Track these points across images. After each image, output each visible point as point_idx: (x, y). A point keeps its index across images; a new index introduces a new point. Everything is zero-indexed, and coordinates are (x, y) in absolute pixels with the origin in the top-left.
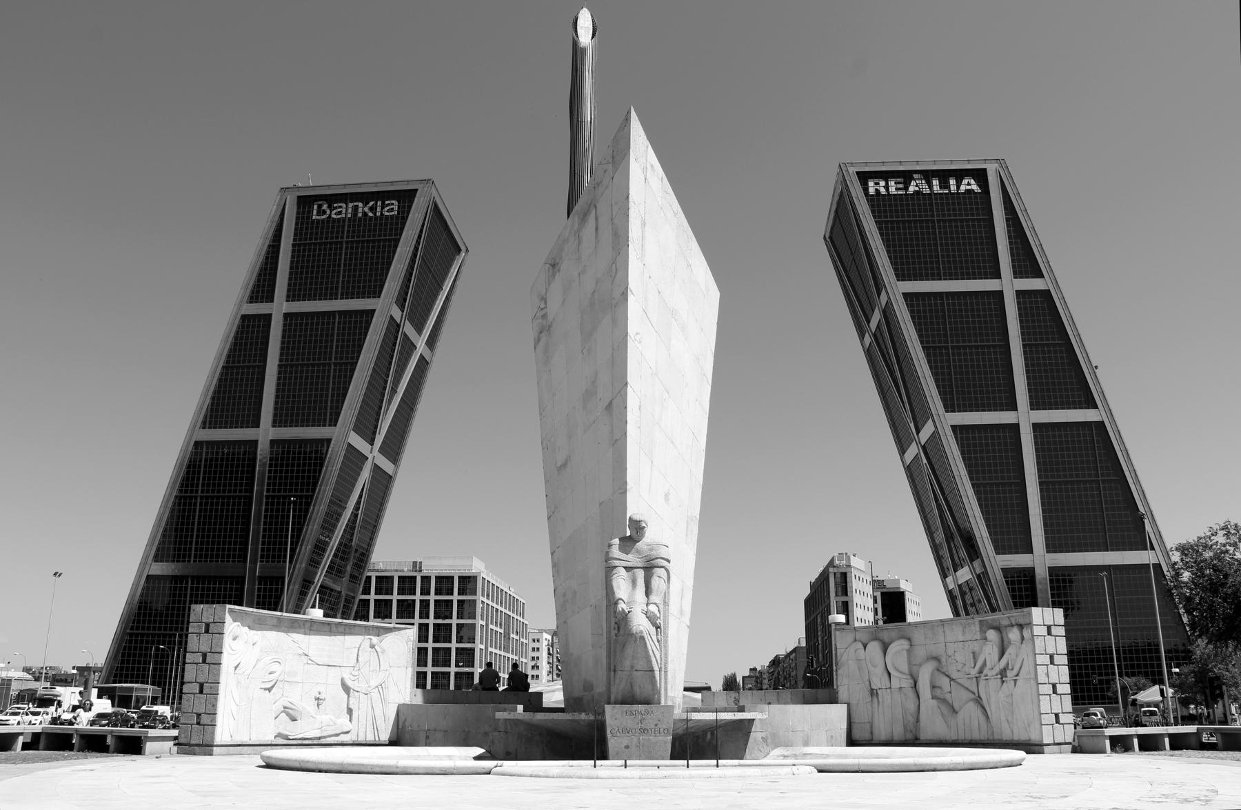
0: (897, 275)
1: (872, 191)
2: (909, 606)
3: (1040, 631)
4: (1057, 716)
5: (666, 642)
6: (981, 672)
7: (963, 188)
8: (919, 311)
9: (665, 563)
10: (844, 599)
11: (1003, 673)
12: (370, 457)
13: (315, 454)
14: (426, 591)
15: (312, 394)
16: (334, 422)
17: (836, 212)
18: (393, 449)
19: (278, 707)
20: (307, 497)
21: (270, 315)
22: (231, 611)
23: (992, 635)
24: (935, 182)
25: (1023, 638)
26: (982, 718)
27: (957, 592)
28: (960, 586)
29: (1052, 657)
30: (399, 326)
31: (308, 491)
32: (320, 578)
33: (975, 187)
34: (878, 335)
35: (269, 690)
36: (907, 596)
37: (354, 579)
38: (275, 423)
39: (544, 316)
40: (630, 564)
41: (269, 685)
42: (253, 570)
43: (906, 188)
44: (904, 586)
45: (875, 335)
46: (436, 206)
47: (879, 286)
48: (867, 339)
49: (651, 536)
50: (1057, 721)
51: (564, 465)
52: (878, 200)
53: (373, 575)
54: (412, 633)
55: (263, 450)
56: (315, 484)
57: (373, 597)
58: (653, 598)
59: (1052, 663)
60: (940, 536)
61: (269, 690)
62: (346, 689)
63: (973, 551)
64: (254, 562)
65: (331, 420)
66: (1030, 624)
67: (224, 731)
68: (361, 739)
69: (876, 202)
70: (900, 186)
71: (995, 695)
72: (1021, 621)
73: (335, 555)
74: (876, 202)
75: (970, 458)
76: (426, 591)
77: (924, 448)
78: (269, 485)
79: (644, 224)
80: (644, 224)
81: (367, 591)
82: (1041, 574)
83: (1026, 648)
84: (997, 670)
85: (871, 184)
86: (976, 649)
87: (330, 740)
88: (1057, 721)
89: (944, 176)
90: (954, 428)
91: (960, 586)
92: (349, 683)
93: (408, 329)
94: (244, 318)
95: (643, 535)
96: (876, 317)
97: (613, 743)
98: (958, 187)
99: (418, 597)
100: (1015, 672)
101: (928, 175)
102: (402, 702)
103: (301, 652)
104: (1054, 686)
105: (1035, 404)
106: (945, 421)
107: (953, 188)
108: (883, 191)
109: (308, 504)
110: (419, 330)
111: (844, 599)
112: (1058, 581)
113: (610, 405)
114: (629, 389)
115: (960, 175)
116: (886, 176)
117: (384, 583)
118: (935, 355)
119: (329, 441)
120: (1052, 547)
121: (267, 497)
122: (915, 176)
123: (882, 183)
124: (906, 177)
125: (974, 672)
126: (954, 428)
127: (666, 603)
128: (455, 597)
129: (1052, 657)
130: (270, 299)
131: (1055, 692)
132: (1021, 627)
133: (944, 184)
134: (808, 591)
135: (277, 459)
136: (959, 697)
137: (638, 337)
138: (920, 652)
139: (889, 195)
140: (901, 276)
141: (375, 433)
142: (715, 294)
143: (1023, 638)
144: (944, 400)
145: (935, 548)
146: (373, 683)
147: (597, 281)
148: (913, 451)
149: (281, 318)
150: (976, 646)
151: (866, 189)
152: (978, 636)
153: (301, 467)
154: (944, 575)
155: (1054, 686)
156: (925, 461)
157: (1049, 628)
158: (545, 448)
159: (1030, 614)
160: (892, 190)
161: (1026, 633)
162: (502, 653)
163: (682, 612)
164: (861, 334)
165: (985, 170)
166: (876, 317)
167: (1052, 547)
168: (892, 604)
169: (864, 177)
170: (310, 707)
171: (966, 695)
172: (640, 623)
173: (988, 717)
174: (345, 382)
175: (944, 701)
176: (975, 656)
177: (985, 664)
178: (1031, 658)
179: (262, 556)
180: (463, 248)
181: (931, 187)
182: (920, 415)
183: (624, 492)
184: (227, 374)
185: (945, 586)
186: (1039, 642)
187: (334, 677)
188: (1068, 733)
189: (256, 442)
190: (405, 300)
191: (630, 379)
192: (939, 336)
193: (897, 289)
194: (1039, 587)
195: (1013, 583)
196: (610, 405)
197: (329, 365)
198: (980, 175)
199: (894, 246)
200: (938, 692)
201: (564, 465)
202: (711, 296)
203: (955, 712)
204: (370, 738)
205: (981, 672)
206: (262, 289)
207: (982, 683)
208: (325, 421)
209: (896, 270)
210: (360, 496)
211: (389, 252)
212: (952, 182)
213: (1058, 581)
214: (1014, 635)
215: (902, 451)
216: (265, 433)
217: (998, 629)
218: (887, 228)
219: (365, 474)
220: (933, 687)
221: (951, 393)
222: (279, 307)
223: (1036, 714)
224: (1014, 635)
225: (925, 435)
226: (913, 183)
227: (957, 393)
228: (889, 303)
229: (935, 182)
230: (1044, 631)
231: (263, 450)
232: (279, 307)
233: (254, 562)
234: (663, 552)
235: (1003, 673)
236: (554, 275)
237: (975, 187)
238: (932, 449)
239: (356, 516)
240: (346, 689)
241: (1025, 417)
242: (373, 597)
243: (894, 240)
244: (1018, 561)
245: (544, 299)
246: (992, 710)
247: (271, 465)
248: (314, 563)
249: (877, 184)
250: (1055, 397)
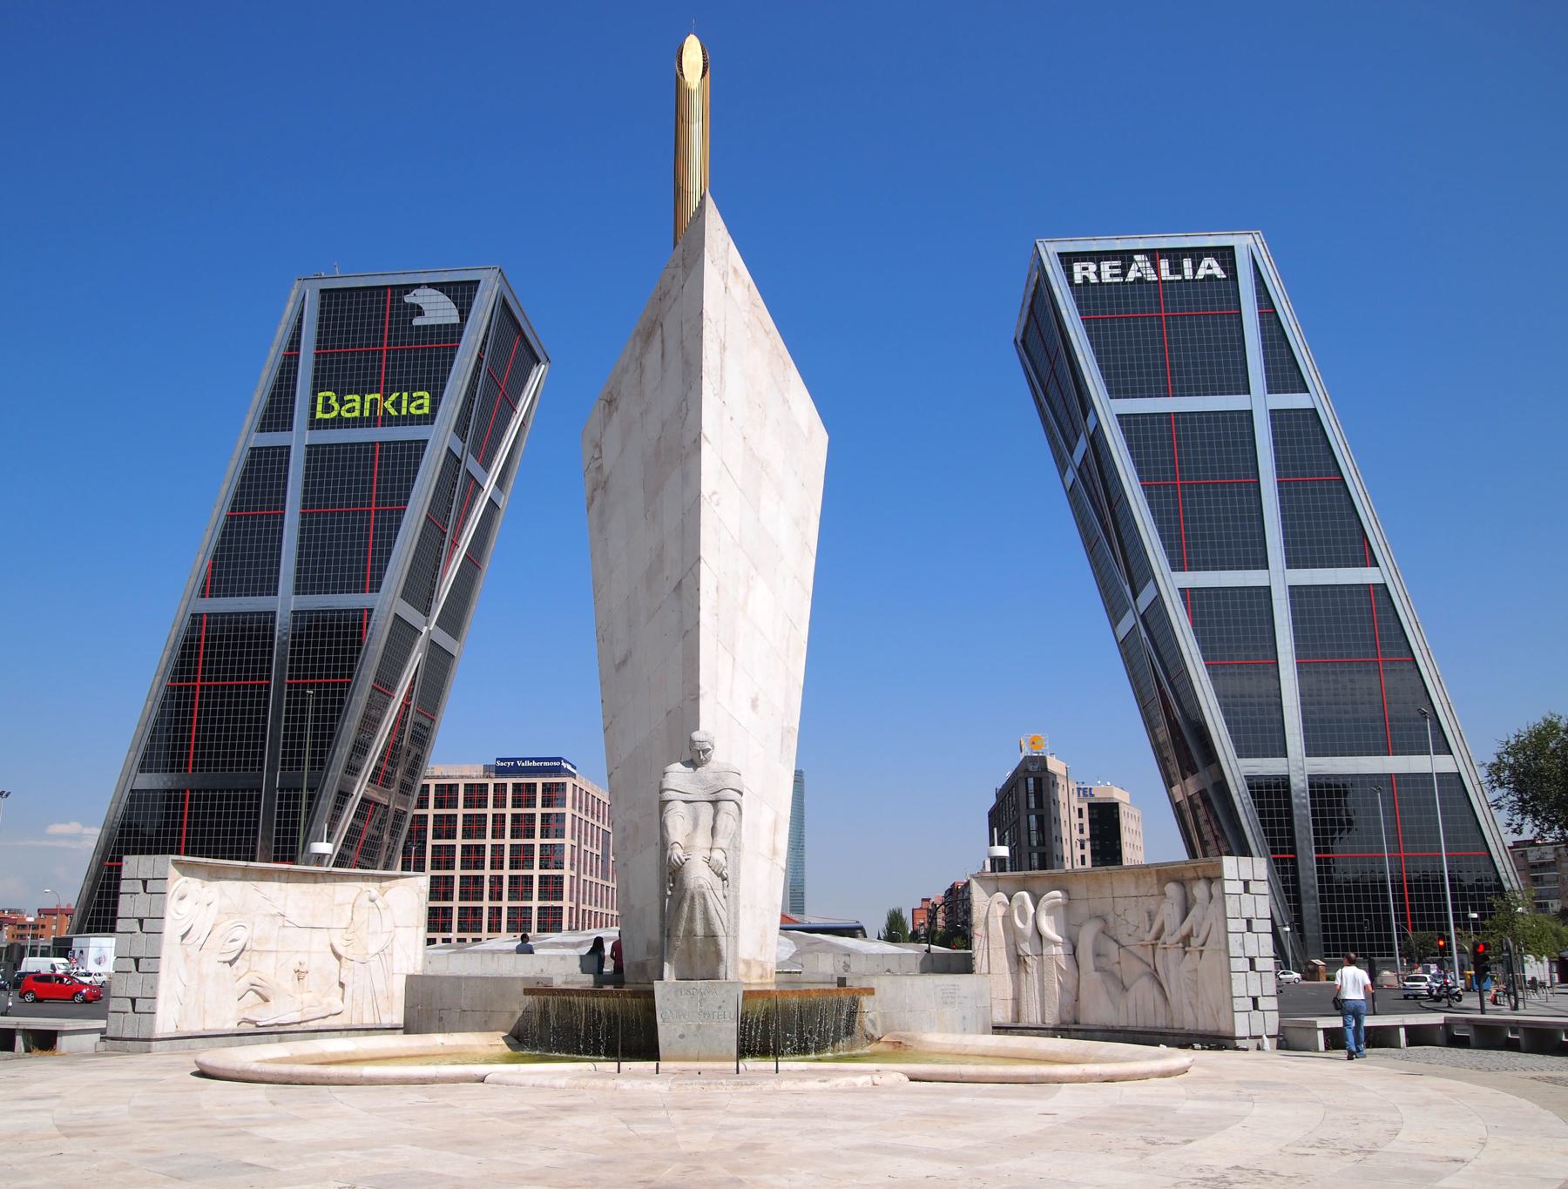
0: (1109, 391)
1: (1078, 279)
2: (1124, 822)
3: (1234, 887)
4: (1255, 1000)
5: (736, 897)
6: (1158, 938)
8: (1138, 439)
9: (736, 796)
10: (1040, 812)
11: (1186, 940)
12: (425, 630)
13: (352, 628)
14: (500, 802)
15: (348, 552)
16: (376, 587)
17: (1031, 306)
18: (453, 621)
19: (244, 983)
20: (342, 685)
21: (289, 447)
22: (176, 863)
23: (1172, 889)
25: (1211, 897)
26: (1159, 999)
27: (1186, 805)
28: (1190, 798)
29: (1249, 922)
30: (459, 461)
31: (342, 676)
32: (361, 788)
34: (1085, 470)
35: (231, 963)
36: (1123, 809)
37: (406, 789)
38: (300, 589)
39: (600, 468)
40: (690, 798)
41: (230, 957)
42: (271, 780)
43: (1124, 275)
44: (1119, 795)
45: (1079, 470)
46: (505, 303)
47: (1086, 404)
48: (1070, 476)
49: (718, 758)
50: (1255, 1007)
51: (624, 662)
52: (1087, 291)
53: (432, 783)
54: (421, 883)
55: (283, 626)
56: (351, 668)
57: (431, 811)
58: (722, 841)
59: (1249, 929)
60: (1163, 734)
61: (231, 963)
62: (338, 957)
63: (1210, 756)
64: (272, 770)
65: (372, 584)
66: (1220, 878)
67: (165, 1023)
68: (355, 1023)
69: (1084, 293)
71: (1175, 969)
72: (1211, 874)
73: (381, 759)
74: (1084, 293)
75: (1203, 632)
76: (500, 802)
77: (1143, 617)
78: (291, 669)
79: (723, 348)
80: (723, 348)
81: (423, 803)
82: (1299, 784)
83: (1214, 908)
84: (1178, 936)
85: (1077, 267)
86: (1153, 907)
87: (313, 1025)
88: (1255, 1007)
90: (1183, 591)
91: (1190, 798)
92: (340, 950)
93: (472, 464)
94: (255, 452)
95: (707, 761)
96: (1082, 445)
97: (666, 1033)
99: (490, 811)
100: (1201, 940)
102: (411, 972)
103: (275, 911)
104: (1252, 960)
105: (1293, 562)
106: (1171, 583)
108: (1093, 279)
109: (342, 694)
110: (487, 466)
111: (1040, 812)
112: (1321, 794)
113: (678, 587)
114: (703, 565)
116: (1097, 257)
117: (446, 794)
118: (1159, 496)
119: (371, 610)
120: (1312, 749)
121: (290, 686)
123: (1092, 267)
125: (1149, 937)
126: (1183, 591)
127: (737, 848)
128: (539, 810)
129: (1249, 922)
130: (287, 425)
131: (1252, 968)
132: (1210, 880)
134: (992, 801)
135: (301, 636)
136: (1132, 969)
137: (715, 498)
138: (1082, 909)
139: (1101, 283)
140: (1115, 392)
141: (430, 600)
142: (821, 439)
143: (1211, 897)
144: (1170, 556)
145: (1158, 748)
146: (373, 949)
147: (664, 425)
148: (1128, 621)
149: (303, 450)
150: (1152, 904)
151: (1070, 276)
152: (1155, 891)
153: (332, 646)
154: (1169, 784)
155: (1252, 960)
156: (1144, 634)
157: (1246, 883)
158: (601, 639)
159: (1220, 866)
160: (1106, 277)
161: (1215, 889)
162: (600, 881)
163: (775, 852)
164: (1062, 471)
165: (1230, 250)
166: (1082, 445)
167: (1312, 749)
168: (1105, 820)
170: (287, 982)
171: (1138, 967)
172: (699, 875)
173: (1166, 998)
174: (389, 536)
175: (1112, 974)
176: (1151, 916)
177: (1162, 929)
178: (1221, 924)
179: (283, 763)
180: (542, 357)
182: (1139, 574)
183: (696, 699)
184: (232, 526)
185: (1171, 797)
186: (1231, 903)
187: (319, 942)
188: (1272, 1023)
189: (274, 613)
190: (467, 427)
191: (704, 553)
192: (1164, 471)
193: (1108, 409)
194: (1295, 801)
195: (1260, 795)
196: (678, 587)
197: (369, 512)
199: (1107, 352)
200: (1104, 960)
201: (624, 662)
202: (815, 441)
203: (1125, 989)
204: (368, 1021)
205: (1158, 938)
206: (277, 414)
207: (1159, 952)
208: (364, 585)
209: (1108, 384)
210: (413, 682)
211: (444, 364)
213: (1321, 794)
214: (1200, 890)
215: (1115, 620)
216: (285, 603)
217: (1181, 882)
218: (1097, 329)
219: (417, 657)
220: (1097, 955)
221: (1180, 546)
222: (299, 439)
223: (1227, 994)
224: (1200, 890)
225: (1144, 600)
227: (1188, 546)
228: (1098, 426)
230: (1239, 887)
231: (283, 626)
232: (299, 439)
233: (272, 770)
234: (732, 782)
235: (1186, 940)
236: (610, 415)
238: (1155, 616)
239: (408, 707)
240: (338, 957)
241: (1279, 577)
242: (431, 811)
243: (1106, 344)
244: (1268, 766)
245: (598, 446)
246: (1172, 988)
247: (293, 644)
248: (353, 770)
249: (1085, 269)
250: (1321, 551)
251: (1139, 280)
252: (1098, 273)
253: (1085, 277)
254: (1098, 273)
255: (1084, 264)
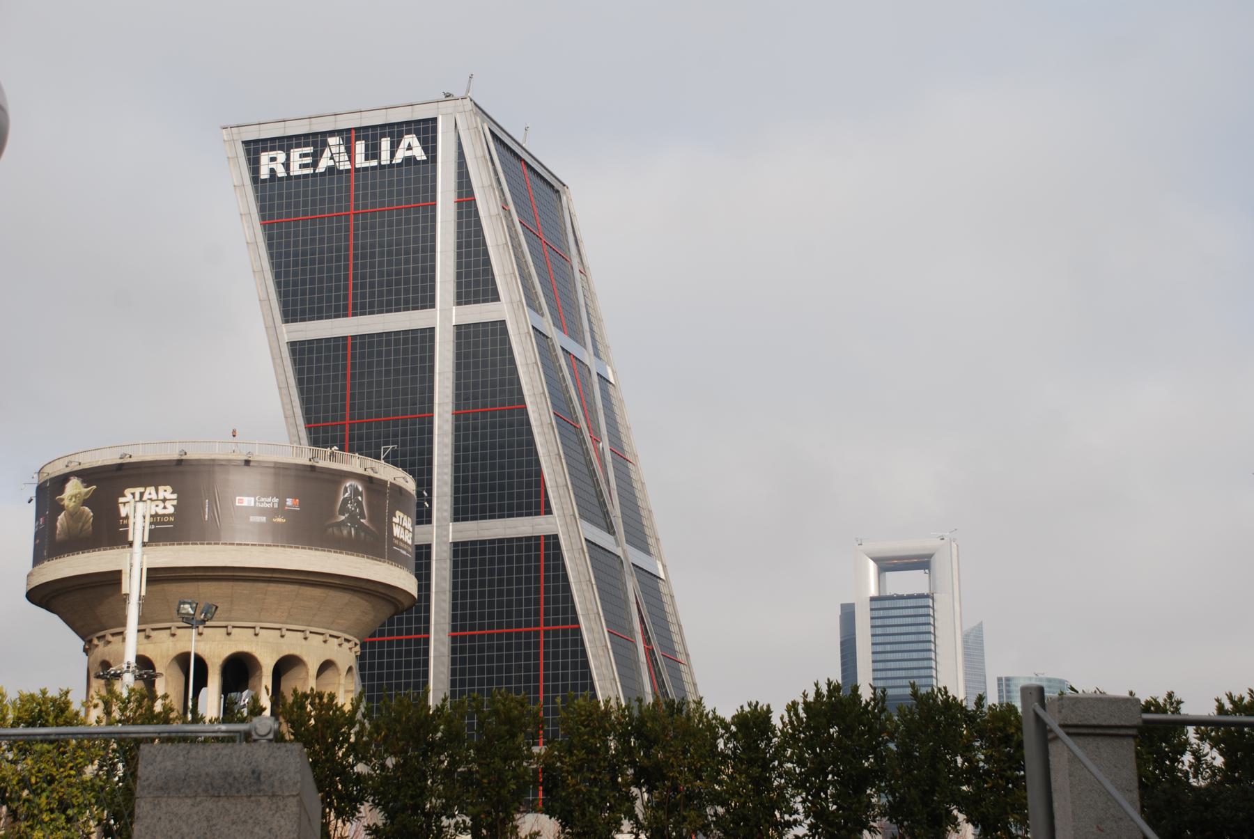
1: (264, 174)
7: (401, 155)
24: (360, 147)
33: (419, 153)
43: (315, 164)
70: (308, 160)
85: (265, 158)
89: (372, 135)
98: (393, 155)
101: (349, 136)
107: (385, 158)
108: (281, 172)
115: (396, 131)
116: (286, 143)
122: (332, 141)
123: (281, 156)
124: (317, 141)
133: (373, 152)
139: (289, 177)
151: (255, 170)
160: (295, 170)
169: (254, 149)
181: (351, 159)
198: (426, 130)
212: (385, 144)
226: (327, 153)
229: (360, 147)
237: (419, 153)
249: (273, 159)
251: (331, 170)
252: (287, 165)
253: (272, 170)
254: (287, 165)
255: (273, 154)
